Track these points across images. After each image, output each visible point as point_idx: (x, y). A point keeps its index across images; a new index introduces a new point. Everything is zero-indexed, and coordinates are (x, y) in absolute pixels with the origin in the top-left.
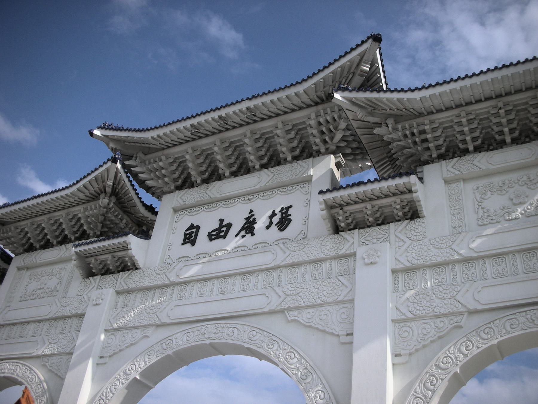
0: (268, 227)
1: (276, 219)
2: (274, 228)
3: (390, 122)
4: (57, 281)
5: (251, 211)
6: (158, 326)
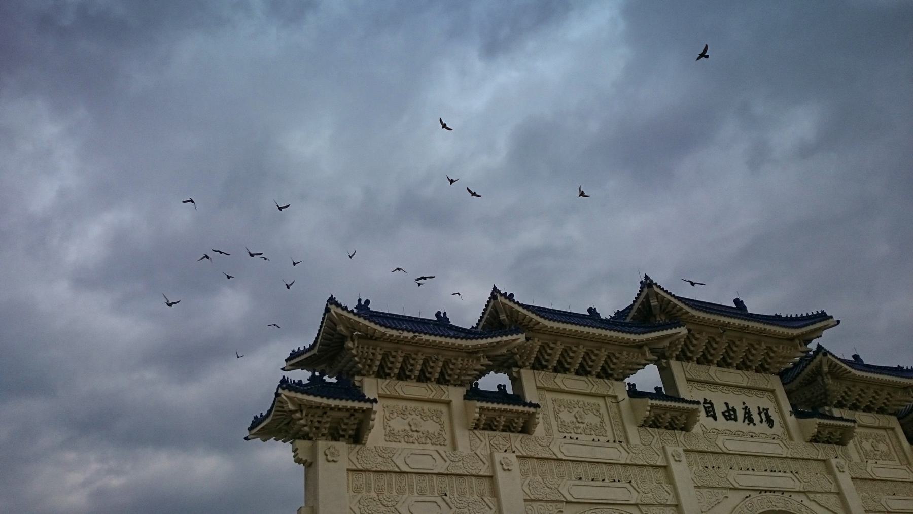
0: (761, 421)
1: (763, 416)
2: (765, 424)
3: (829, 377)
5: (744, 403)
6: (731, 489)
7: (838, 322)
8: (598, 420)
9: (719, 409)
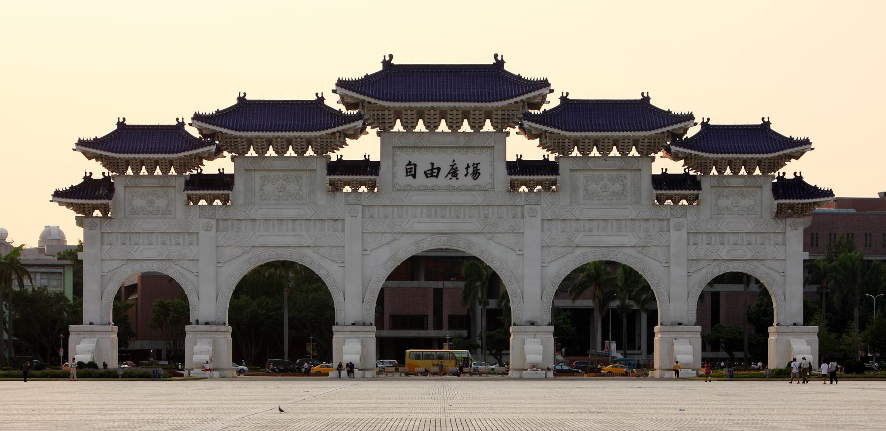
0: (466, 176)
1: (471, 170)
2: (470, 177)
4: (298, 187)
7: (552, 91)
8: (298, 187)
9: (423, 166)
